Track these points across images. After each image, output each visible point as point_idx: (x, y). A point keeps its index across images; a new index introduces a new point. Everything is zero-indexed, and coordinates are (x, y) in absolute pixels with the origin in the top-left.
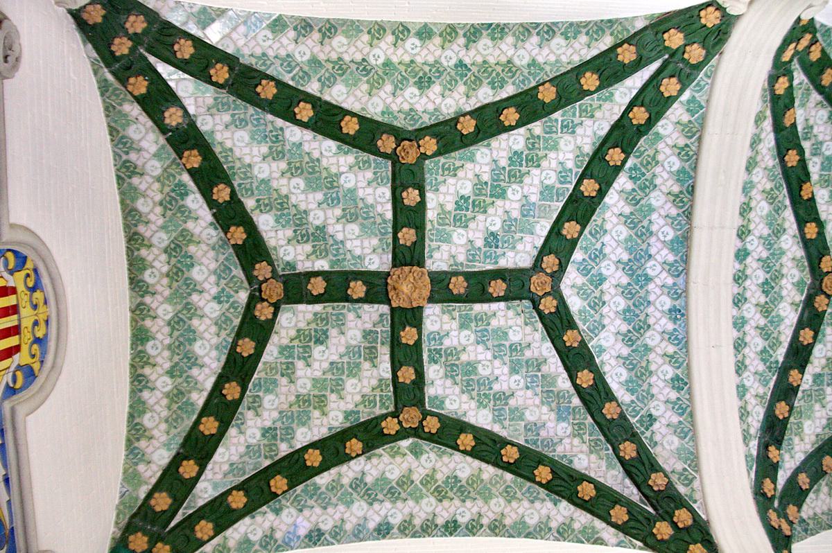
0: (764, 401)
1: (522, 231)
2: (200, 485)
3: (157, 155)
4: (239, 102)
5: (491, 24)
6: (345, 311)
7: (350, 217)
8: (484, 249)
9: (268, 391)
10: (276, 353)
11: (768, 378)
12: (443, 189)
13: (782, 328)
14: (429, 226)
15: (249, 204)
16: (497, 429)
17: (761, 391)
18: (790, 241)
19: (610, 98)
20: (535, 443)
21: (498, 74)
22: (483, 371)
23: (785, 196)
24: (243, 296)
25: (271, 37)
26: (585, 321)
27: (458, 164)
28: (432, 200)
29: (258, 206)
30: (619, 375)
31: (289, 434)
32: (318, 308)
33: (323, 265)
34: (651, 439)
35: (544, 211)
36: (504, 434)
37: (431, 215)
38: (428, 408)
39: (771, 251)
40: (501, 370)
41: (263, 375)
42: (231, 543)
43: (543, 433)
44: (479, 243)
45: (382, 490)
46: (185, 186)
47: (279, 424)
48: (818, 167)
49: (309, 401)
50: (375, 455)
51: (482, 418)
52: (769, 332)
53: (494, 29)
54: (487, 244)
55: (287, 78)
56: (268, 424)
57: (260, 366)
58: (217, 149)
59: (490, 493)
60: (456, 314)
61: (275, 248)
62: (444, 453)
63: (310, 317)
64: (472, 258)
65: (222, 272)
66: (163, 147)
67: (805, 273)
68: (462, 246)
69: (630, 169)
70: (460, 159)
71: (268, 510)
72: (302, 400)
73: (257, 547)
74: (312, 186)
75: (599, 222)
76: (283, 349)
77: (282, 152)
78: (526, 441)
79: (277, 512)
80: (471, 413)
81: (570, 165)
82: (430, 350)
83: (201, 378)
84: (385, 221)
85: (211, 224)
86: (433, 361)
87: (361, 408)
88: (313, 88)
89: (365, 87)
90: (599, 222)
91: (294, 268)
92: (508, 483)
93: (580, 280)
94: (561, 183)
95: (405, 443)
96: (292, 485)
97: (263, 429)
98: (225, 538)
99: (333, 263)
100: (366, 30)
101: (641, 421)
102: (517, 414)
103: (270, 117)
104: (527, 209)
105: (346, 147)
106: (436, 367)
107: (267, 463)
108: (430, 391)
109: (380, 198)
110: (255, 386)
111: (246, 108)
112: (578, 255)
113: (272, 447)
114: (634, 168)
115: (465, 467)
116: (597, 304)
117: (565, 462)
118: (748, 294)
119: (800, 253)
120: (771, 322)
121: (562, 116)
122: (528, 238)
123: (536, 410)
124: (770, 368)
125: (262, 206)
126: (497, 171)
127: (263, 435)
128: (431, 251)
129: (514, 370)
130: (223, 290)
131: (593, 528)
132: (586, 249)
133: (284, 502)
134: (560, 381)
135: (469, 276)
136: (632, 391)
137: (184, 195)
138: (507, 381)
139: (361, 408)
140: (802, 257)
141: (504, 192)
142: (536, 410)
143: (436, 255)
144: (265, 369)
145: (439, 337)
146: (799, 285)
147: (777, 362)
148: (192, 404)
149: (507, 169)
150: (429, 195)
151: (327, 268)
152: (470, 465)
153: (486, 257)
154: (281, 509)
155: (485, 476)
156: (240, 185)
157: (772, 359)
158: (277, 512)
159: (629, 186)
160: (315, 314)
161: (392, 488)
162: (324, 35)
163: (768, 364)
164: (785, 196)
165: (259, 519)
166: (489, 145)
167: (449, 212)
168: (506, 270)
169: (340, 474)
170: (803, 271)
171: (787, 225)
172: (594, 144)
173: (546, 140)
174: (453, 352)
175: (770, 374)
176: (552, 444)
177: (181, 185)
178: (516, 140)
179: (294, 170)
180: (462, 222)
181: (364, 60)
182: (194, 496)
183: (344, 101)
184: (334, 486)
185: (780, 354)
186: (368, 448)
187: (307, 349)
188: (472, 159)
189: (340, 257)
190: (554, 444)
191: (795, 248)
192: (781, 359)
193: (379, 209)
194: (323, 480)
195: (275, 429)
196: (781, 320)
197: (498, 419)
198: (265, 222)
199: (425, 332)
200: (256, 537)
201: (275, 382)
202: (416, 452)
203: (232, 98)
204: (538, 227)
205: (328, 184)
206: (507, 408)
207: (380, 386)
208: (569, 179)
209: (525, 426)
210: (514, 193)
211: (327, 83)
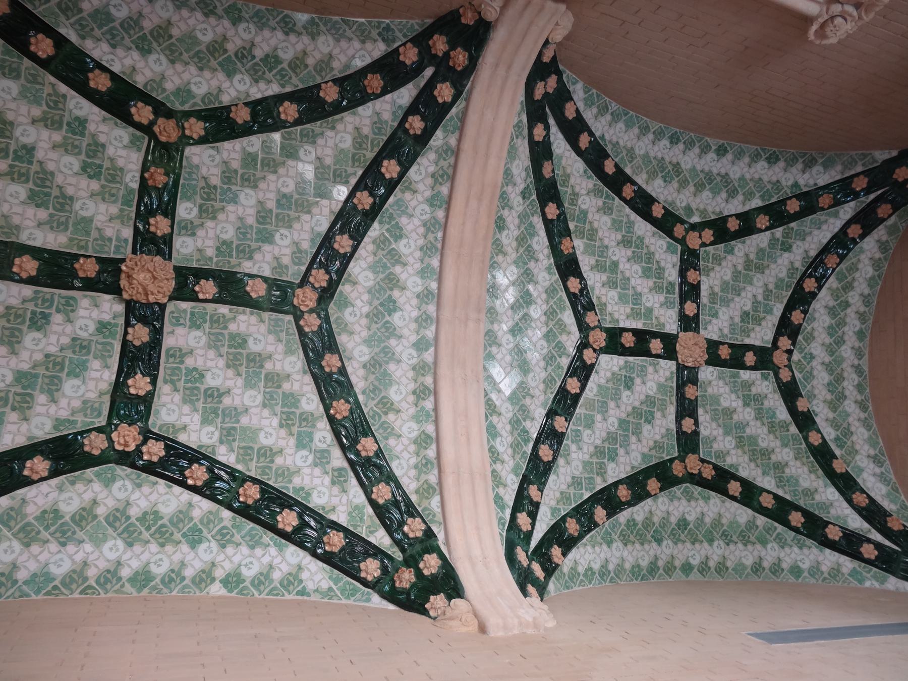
0: (407, 184)
1: (607, 388)
2: (848, 217)
3: (861, 470)
4: (812, 510)
5: (642, 579)
6: (729, 336)
7: (729, 412)
8: (634, 375)
9: (782, 280)
10: (775, 310)
11: (395, 208)
12: (663, 431)
13: (371, 259)
14: (674, 399)
15: (793, 429)
16: (634, 216)
17: (408, 196)
18: (356, 353)
19: (554, 511)
20: (607, 197)
21: (632, 533)
22: (637, 268)
23: (366, 406)
24: (796, 356)
25: (799, 563)
26: (560, 299)
27: (653, 453)
28: (670, 421)
29: (787, 426)
30: (538, 243)
31: (773, 242)
32: (747, 341)
33: (745, 375)
34: (528, 174)
35: (590, 405)
36: (628, 210)
37: (672, 410)
38: (679, 247)
39: (382, 345)
40: (623, 266)
41: (784, 293)
42: (839, 168)
43: (600, 203)
44: (638, 381)
45: (716, 184)
46: (838, 446)
47: (779, 252)
48: (318, 436)
49: (756, 268)
50: (717, 215)
51: (642, 227)
52: (388, 257)
53: (639, 575)
54: (632, 379)
55: (780, 528)
56: (786, 255)
57: (785, 301)
58: (820, 472)
59: (644, 160)
60: (654, 322)
61: (775, 391)
62: (670, 205)
63: (752, 335)
64: (643, 369)
65: (810, 376)
66: (858, 476)
67: (336, 316)
68: (650, 380)
69: (529, 441)
70: (651, 456)
71: (802, 187)
72: (760, 269)
73: (820, 161)
74: (753, 440)
75: (549, 391)
76: (770, 311)
77: (775, 468)
78: (613, 199)
79: (796, 185)
80: (650, 234)
81: (573, 447)
82: (674, 294)
83: (829, 298)
84: (703, 406)
85: (816, 415)
86: (671, 284)
87: (723, 255)
88: (761, 520)
89: (724, 521)
90: (549, 391)
91: (762, 374)
92: (629, 166)
93: (563, 338)
94: (579, 431)
95: (695, 219)
96: (783, 202)
97: (790, 252)
98: (842, 173)
99: (736, 376)
100: (730, 570)
101: (531, 195)
102: (617, 225)
103: (788, 497)
104: (604, 409)
105: (732, 470)
106: (671, 279)
107: (793, 225)
108: (676, 259)
109: (708, 427)
110: (790, 286)
111: (805, 504)
112: (565, 362)
113: (786, 235)
114: (526, 441)
115: (656, 188)
116: (550, 314)
117: (590, 172)
118: (415, 302)
119: (342, 339)
120: (385, 267)
121: (582, 494)
122: (603, 381)
123: (602, 223)
124: (391, 217)
125: (784, 426)
126: (626, 445)
127: (791, 246)
128: (672, 378)
129: (615, 264)
130: (808, 363)
131: (586, 104)
132: (559, 367)
133: (789, 192)
134: (582, 248)
135: (647, 353)
136: (532, 226)
137: (837, 439)
138: (620, 254)
139: (723, 255)
140: (340, 334)
141: (620, 425)
142: (602, 223)
143: (668, 374)
144: (783, 298)
145: (667, 304)
146: (346, 303)
147: (380, 223)
148: (837, 279)
149: (618, 446)
150: (673, 426)
151: (742, 372)
152: (654, 189)
153: (633, 368)
154: (792, 186)
155: (644, 176)
156: (801, 444)
157: (387, 226)
158: (796, 185)
159: (528, 424)
160: (748, 336)
161: (710, 184)
162: (760, 565)
163: (393, 223)
164: (366, 406)
165: (811, 182)
166: (633, 468)
167: (658, 410)
168: (620, 355)
169: (744, 204)
170: (337, 318)
171: (361, 372)
172: (558, 467)
173: (592, 471)
174: (657, 289)
175: (391, 211)
176: (596, 192)
177: (841, 447)
178: (616, 471)
179: (766, 453)
180: (649, 401)
181: (728, 545)
182: (855, 209)
183: (737, 509)
184: (749, 196)
185: (376, 230)
186: (724, 219)
187: (755, 309)
188: (644, 456)
189: (732, 380)
190: (594, 190)
191: (350, 345)
192: (376, 225)
193: (708, 417)
194: (756, 203)
195: (781, 250)
196: (372, 268)
197: (630, 224)
198: (783, 414)
199: (677, 309)
200: (817, 168)
201: (777, 287)
202: (689, 210)
203: (816, 513)
204: (595, 390)
205: (745, 442)
206: (624, 233)
207: (709, 271)
208: (574, 434)
209: (611, 214)
210: (613, 423)
211: (751, 525)
